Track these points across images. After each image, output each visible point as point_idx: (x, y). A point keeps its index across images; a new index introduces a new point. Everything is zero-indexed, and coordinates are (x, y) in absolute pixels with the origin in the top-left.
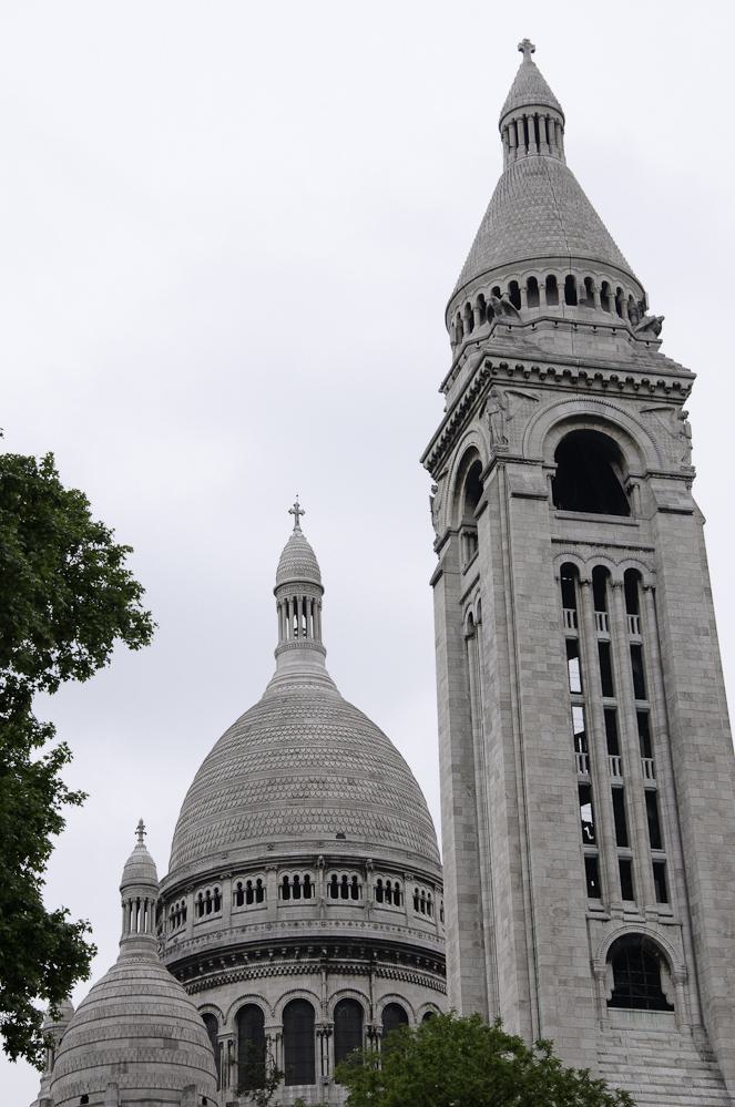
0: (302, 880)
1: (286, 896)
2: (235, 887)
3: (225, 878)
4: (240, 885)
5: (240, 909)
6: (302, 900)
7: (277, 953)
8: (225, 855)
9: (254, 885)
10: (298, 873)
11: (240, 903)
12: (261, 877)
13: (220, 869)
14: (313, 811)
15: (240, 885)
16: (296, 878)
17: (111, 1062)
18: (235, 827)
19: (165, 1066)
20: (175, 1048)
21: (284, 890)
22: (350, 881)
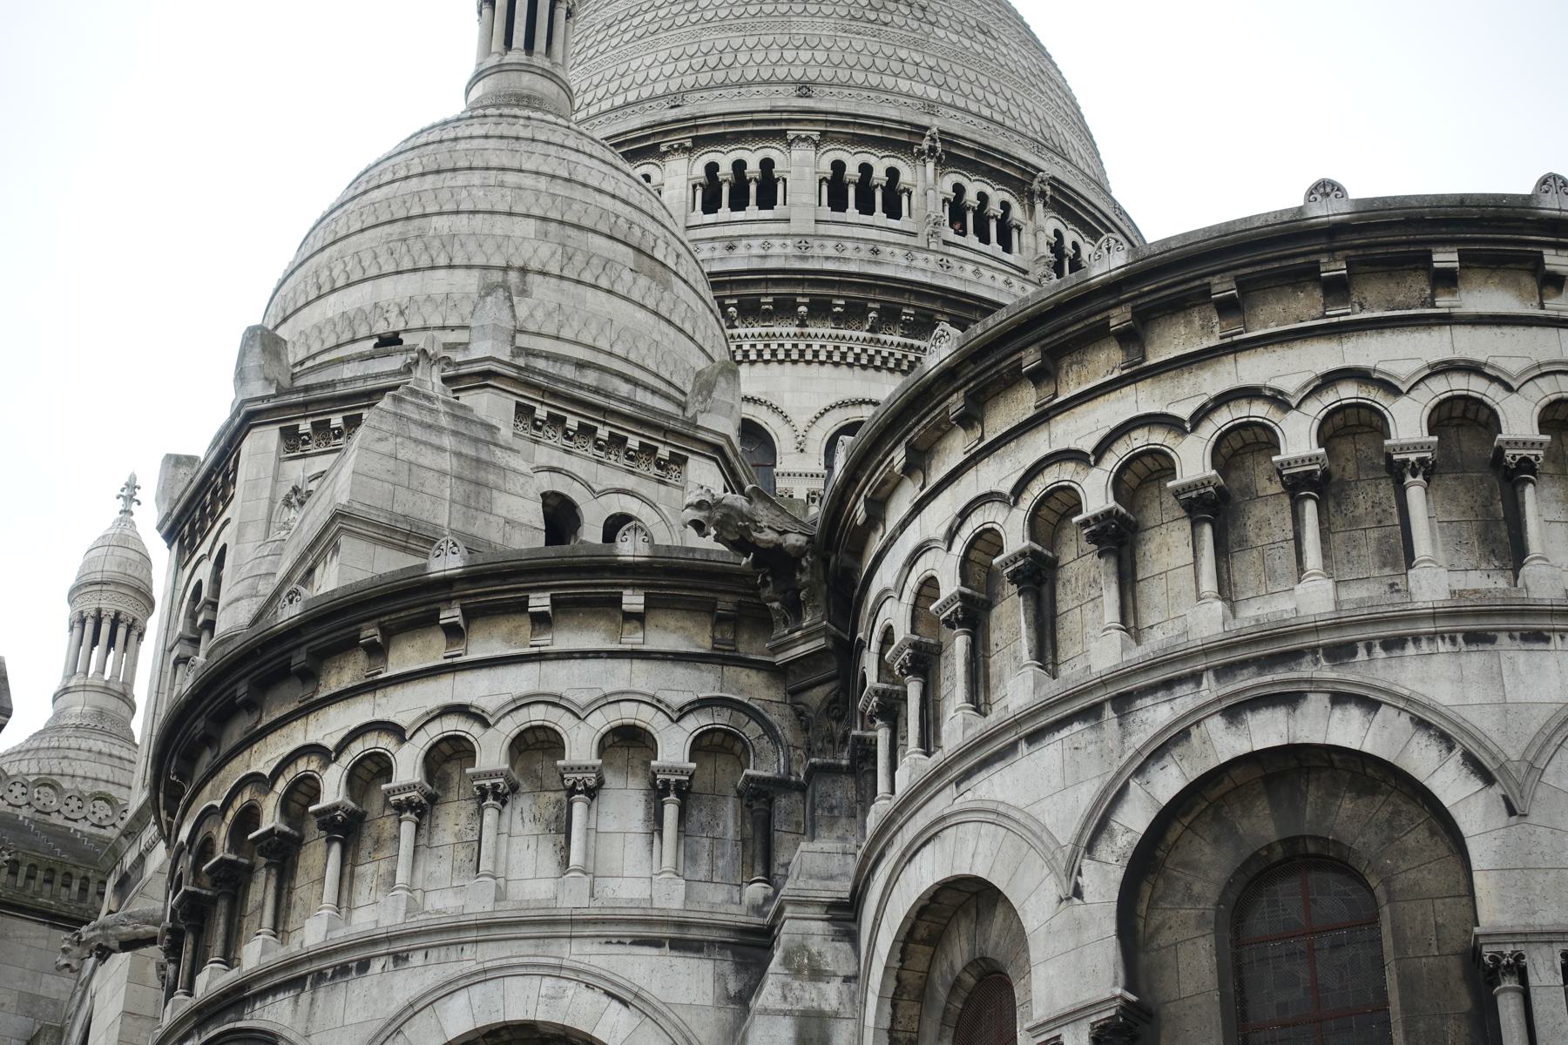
0: (879, 175)
1: (838, 203)
2: (699, 171)
3: (672, 150)
4: (712, 168)
5: (710, 218)
6: (879, 217)
7: (821, 309)
8: (675, 98)
9: (753, 168)
10: (872, 160)
11: (711, 205)
12: (773, 154)
13: (663, 129)
14: (903, 54)
15: (712, 168)
16: (866, 169)
17: (479, 260)
18: (697, 62)
19: (641, 315)
20: (666, 286)
21: (835, 189)
22: (994, 208)
